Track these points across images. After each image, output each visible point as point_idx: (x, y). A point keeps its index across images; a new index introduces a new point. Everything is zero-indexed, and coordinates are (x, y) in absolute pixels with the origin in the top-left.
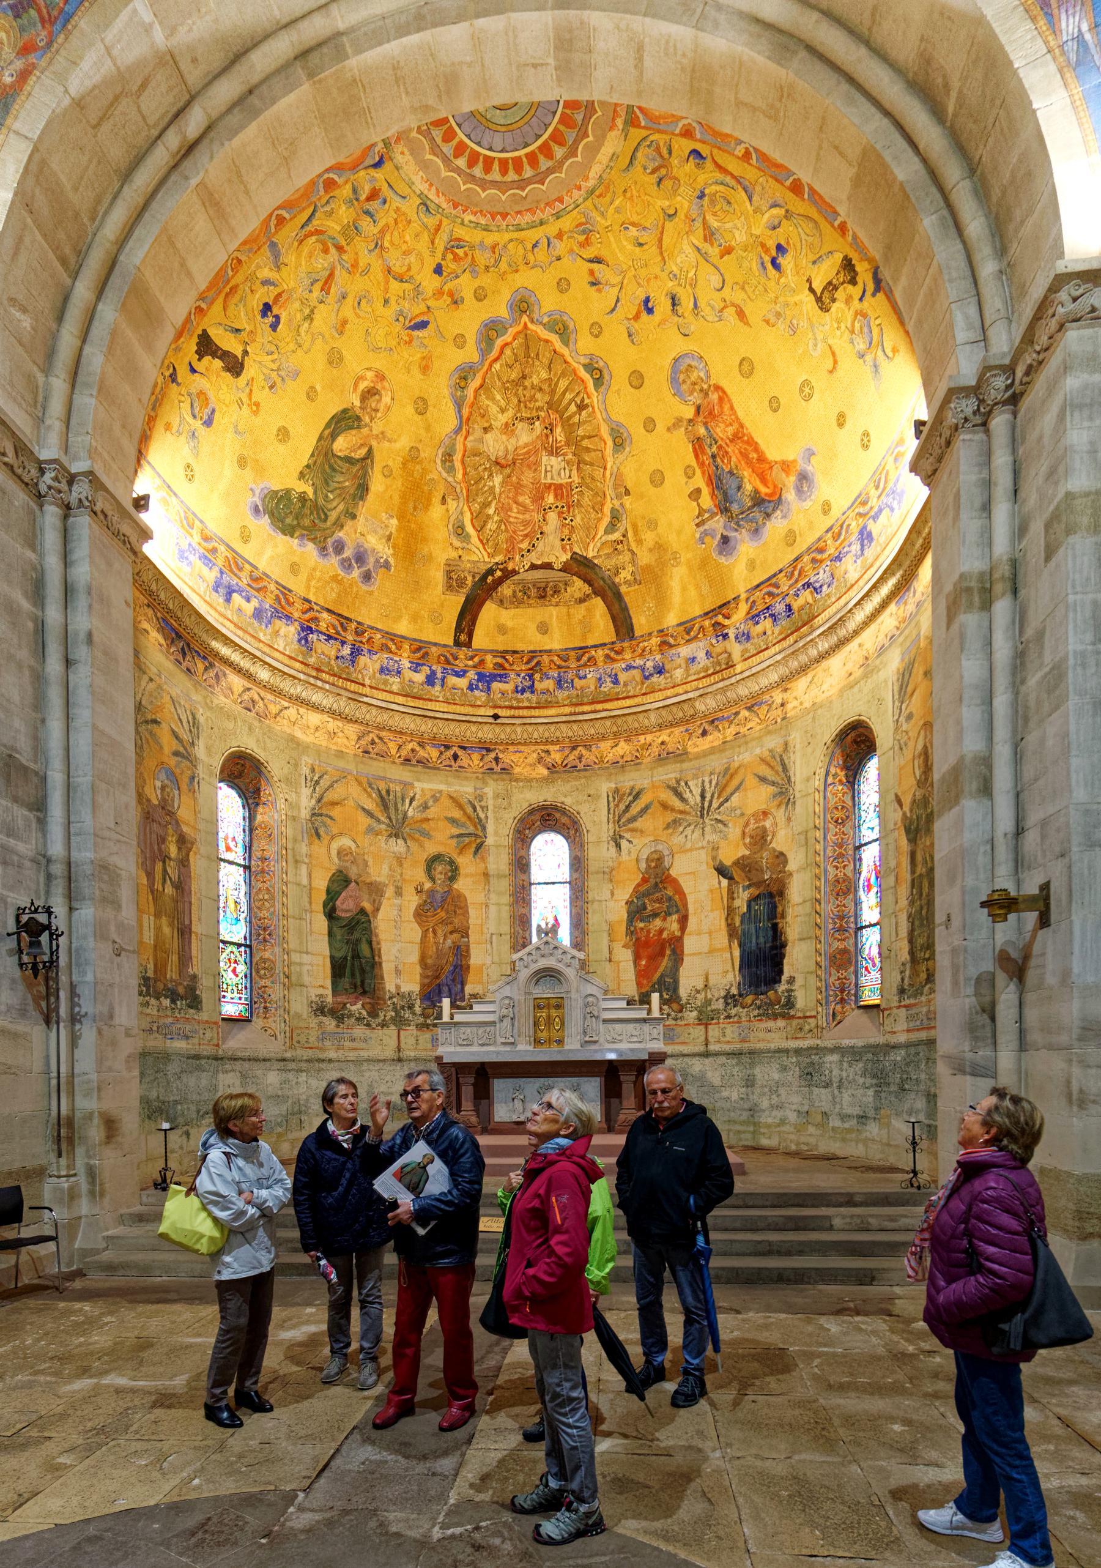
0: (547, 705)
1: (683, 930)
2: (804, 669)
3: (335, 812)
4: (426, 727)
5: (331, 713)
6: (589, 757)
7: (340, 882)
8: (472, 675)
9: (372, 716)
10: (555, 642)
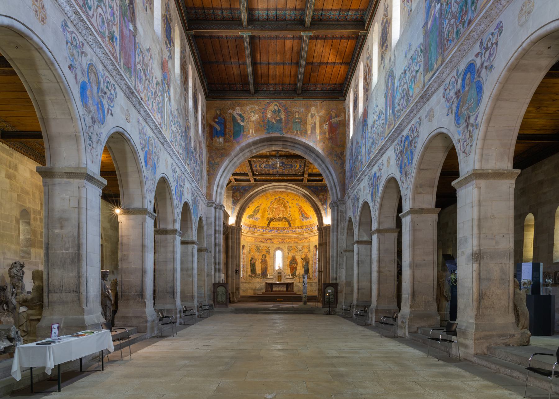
0: (279, 234)
1: (297, 266)
2: (312, 236)
3: (251, 250)
4: (262, 237)
5: (251, 237)
6: (285, 241)
7: (252, 259)
8: (269, 230)
9: (256, 236)
10: (281, 226)
